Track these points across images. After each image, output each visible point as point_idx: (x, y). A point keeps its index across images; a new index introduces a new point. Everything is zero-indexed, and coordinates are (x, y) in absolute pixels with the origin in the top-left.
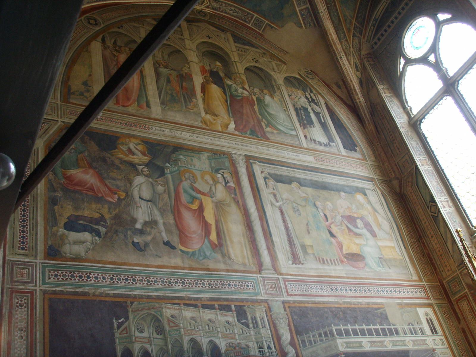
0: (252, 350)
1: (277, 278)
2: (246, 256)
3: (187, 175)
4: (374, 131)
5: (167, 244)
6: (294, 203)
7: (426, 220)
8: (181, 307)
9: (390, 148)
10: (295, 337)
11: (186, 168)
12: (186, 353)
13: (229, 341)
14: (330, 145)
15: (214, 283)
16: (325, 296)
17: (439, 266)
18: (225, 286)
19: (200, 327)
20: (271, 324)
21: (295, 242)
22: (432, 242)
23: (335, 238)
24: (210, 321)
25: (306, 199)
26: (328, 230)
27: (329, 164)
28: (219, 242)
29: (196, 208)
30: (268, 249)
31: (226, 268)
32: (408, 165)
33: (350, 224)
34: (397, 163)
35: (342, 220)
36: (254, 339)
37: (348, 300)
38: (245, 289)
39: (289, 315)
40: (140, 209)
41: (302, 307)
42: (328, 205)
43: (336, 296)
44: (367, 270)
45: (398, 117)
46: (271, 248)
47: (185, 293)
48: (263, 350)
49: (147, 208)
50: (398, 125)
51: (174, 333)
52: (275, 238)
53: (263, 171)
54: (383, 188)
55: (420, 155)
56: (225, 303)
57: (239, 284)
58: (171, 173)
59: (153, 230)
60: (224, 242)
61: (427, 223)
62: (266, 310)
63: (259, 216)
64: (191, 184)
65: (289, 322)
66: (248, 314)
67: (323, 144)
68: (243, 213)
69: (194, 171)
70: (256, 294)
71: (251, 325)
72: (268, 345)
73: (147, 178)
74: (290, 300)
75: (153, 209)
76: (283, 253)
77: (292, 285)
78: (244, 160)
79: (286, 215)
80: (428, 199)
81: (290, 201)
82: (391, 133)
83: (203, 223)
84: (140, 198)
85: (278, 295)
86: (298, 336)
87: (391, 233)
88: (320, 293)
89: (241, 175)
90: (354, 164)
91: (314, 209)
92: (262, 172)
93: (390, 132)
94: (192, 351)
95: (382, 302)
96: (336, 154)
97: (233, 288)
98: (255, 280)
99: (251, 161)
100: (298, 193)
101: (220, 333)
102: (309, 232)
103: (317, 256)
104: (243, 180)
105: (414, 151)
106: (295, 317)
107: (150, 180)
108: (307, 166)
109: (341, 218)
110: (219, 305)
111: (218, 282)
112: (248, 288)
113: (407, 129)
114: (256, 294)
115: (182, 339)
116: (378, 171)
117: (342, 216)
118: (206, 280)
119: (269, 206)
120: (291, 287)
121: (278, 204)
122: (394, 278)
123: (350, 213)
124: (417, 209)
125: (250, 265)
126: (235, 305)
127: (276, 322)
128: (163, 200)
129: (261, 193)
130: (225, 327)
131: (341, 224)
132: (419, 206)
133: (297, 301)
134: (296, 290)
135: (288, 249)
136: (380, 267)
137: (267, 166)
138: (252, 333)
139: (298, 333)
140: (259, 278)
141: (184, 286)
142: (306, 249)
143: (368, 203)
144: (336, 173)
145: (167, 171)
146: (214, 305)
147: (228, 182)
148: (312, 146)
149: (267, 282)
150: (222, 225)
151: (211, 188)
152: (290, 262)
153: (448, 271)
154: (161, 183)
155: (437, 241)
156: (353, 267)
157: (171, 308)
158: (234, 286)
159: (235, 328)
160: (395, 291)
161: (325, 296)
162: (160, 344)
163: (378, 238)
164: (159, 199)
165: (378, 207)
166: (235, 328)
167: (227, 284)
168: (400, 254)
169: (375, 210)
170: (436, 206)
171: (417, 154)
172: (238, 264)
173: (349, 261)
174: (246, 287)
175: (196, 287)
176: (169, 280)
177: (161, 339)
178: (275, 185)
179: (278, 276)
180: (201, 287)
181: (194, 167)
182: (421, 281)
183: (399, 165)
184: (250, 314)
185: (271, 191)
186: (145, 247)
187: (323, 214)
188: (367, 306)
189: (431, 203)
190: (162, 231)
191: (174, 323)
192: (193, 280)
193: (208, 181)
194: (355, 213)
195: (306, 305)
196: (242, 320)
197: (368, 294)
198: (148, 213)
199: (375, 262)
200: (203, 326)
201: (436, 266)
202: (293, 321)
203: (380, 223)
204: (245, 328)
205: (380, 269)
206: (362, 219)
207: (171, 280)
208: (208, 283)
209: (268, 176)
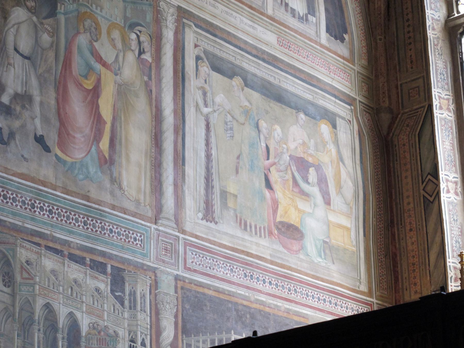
0: (121, 341)
1: (176, 236)
2: (143, 190)
3: (88, 23)
4: (383, 12)
5: (40, 140)
6: (229, 113)
7: (411, 199)
8: (41, 250)
9: (398, 54)
10: (180, 337)
11: (88, 10)
12: (36, 324)
13: (94, 319)
14: (307, 20)
15: (92, 223)
16: (234, 283)
17: (404, 281)
18: (105, 231)
19: (61, 288)
20: (153, 308)
21: (214, 183)
22: (408, 238)
23: (271, 191)
24: (75, 283)
25: (247, 112)
27: (295, 56)
28: (110, 156)
29: (90, 88)
30: (176, 185)
31: (112, 202)
32: (417, 96)
33: (299, 173)
34: (401, 85)
36: (126, 325)
37: (263, 298)
38: (131, 243)
39: (180, 300)
40: (12, 69)
41: (198, 292)
42: (275, 130)
43: (248, 288)
44: (302, 256)
45: (433, 6)
46: (179, 184)
47: (50, 228)
48: (135, 345)
49: (23, 70)
50: (427, 21)
51: (26, 290)
52: (189, 170)
53: (198, 44)
54: (364, 122)
55: (442, 88)
56: (101, 259)
57: (124, 233)
58: (65, 14)
59: (25, 111)
60: (117, 158)
61: (412, 205)
62: (151, 284)
63: (174, 125)
64: (90, 42)
65: (177, 311)
66: (127, 284)
67: (297, 16)
68: (154, 114)
69: (99, 18)
70: (144, 255)
71: (127, 303)
72: (143, 340)
73: (30, 14)
74: (186, 278)
75: (30, 74)
76: (194, 197)
77: (194, 253)
78: (175, 17)
79: (212, 134)
80: (428, 167)
81: (225, 109)
82: (411, 29)
83: (94, 116)
84: (16, 50)
85: (172, 264)
86: (184, 336)
87: (353, 204)
88: (229, 276)
89: (165, 44)
90: (334, 65)
91: (254, 134)
92: (196, 46)
93: (409, 26)
94: (44, 324)
95: (307, 314)
96: (311, 40)
97: (115, 238)
98: (147, 231)
100: (239, 97)
101: (84, 305)
102: (237, 172)
103: (239, 215)
104: (165, 54)
105: (437, 78)
106: (187, 306)
107: (35, 19)
108: (264, 52)
109: (288, 158)
110: (91, 260)
111: (97, 222)
112: (135, 243)
113: (438, 35)
114: (144, 255)
115: (34, 301)
116: (365, 88)
117: (290, 156)
118: (82, 214)
119: (193, 110)
120: (193, 256)
121: (206, 110)
122: (335, 280)
123: (304, 153)
124: (404, 175)
125: (145, 206)
126: (112, 266)
127: (160, 306)
128: (46, 61)
129: (187, 84)
130: (93, 296)
131: (287, 170)
132: (409, 173)
133: (195, 280)
134: (198, 263)
135: (203, 192)
137: (206, 37)
138: (126, 315)
139: (186, 332)
140: (153, 229)
141: (51, 216)
142: (226, 200)
143: (333, 143)
144: (302, 76)
145: (61, 9)
146: (84, 258)
147: (144, 52)
148: (281, 15)
149: (162, 241)
150: (121, 127)
151: (117, 56)
152: (200, 215)
153: (416, 292)
154: (49, 28)
155: (416, 239)
156: (284, 247)
157: (28, 249)
158: (116, 235)
159: (105, 301)
160: (330, 302)
161: (234, 283)
162: (5, 301)
163: (332, 208)
164: (41, 59)
165: (347, 154)
166: (105, 301)
167: (109, 228)
168: (354, 243)
169: (341, 159)
170: (437, 185)
171: (440, 84)
172: (129, 199)
173: (281, 236)
174: (132, 240)
175: (66, 222)
176: (33, 202)
177: (8, 294)
178: (209, 75)
179: (178, 234)
180: (72, 224)
181: (101, 11)
182: (371, 296)
183: (402, 90)
184: (129, 285)
185: (200, 85)
186: (8, 138)
187: (265, 145)
188: (285, 315)
189: (429, 177)
190: (36, 117)
191: (28, 273)
192: (64, 211)
193: (116, 41)
194: (311, 155)
195: (206, 291)
196: (117, 292)
197: (292, 296)
198: (23, 79)
199: (316, 246)
200: (66, 287)
201: (400, 277)
202: (183, 311)
203: (342, 183)
204: (118, 305)
205: (320, 260)
206: (318, 168)
207: (35, 202)
208: (83, 220)
209: (202, 55)
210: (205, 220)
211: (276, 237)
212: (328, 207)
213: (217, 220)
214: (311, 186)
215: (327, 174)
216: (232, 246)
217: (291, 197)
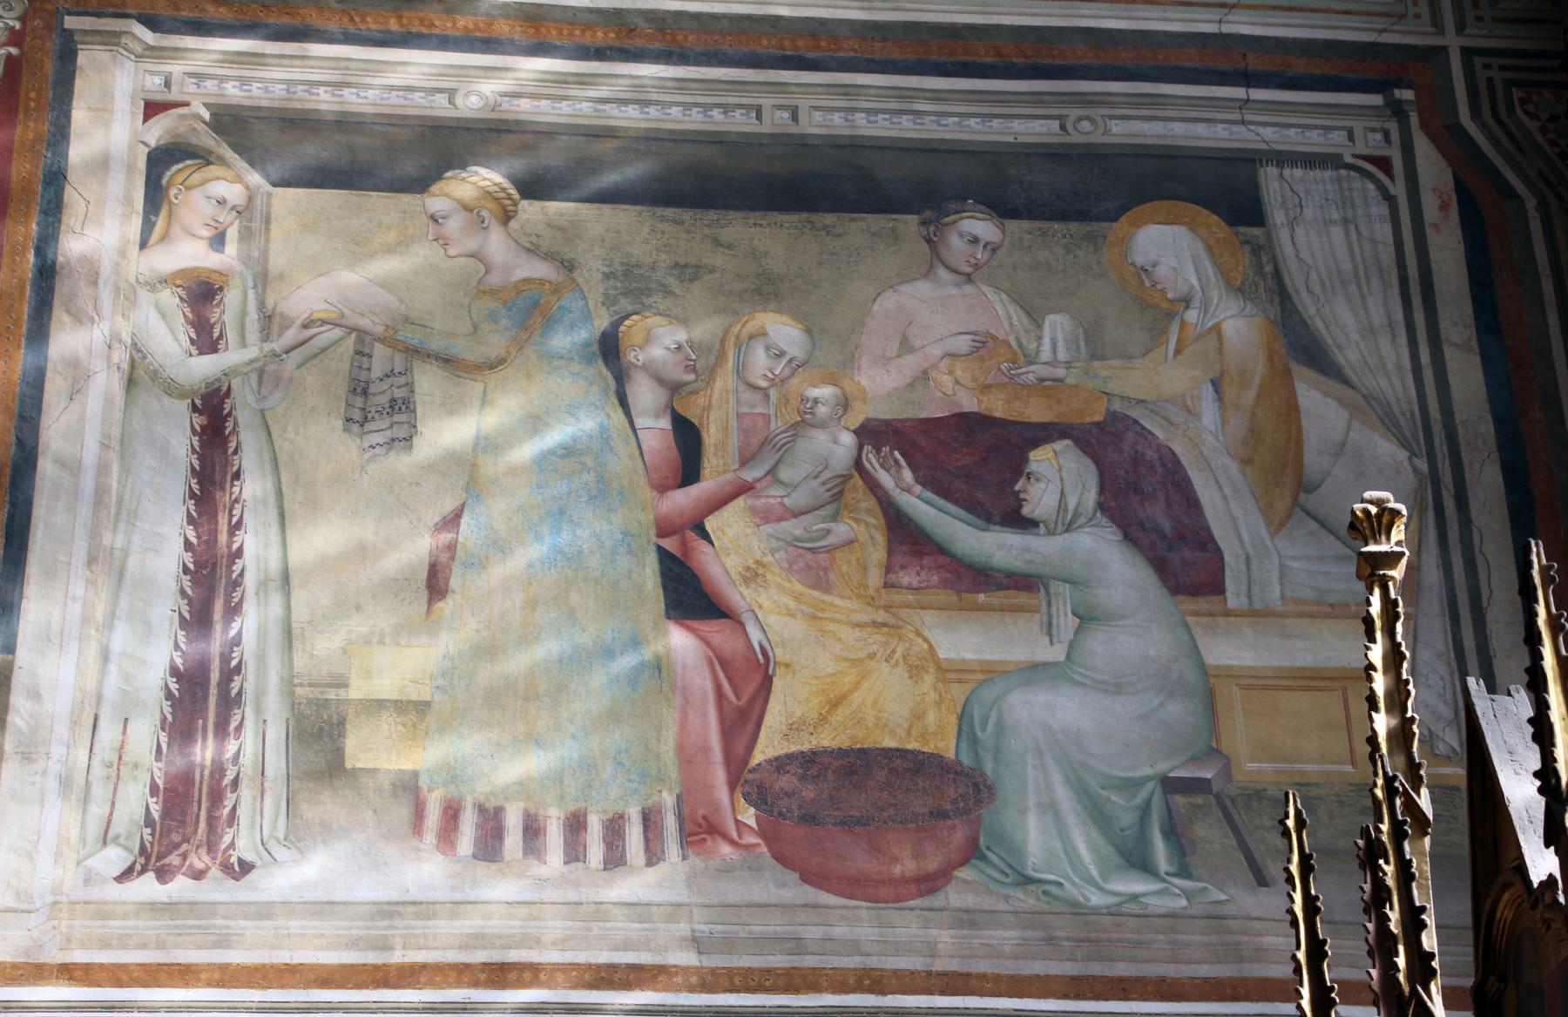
23: (713, 628)
26: (664, 555)
35: (858, 464)
99: (70, 22)
136: (1141, 863)
152: (115, 858)
163: (1234, 596)
187: (665, 423)
203: (1314, 460)
205: (1138, 885)
209: (208, 140)
210: (151, 876)
211: (752, 839)
212: (1203, 604)
213: (249, 857)
214: (1051, 533)
215: (1178, 448)
216: (372, 958)
217: (881, 616)
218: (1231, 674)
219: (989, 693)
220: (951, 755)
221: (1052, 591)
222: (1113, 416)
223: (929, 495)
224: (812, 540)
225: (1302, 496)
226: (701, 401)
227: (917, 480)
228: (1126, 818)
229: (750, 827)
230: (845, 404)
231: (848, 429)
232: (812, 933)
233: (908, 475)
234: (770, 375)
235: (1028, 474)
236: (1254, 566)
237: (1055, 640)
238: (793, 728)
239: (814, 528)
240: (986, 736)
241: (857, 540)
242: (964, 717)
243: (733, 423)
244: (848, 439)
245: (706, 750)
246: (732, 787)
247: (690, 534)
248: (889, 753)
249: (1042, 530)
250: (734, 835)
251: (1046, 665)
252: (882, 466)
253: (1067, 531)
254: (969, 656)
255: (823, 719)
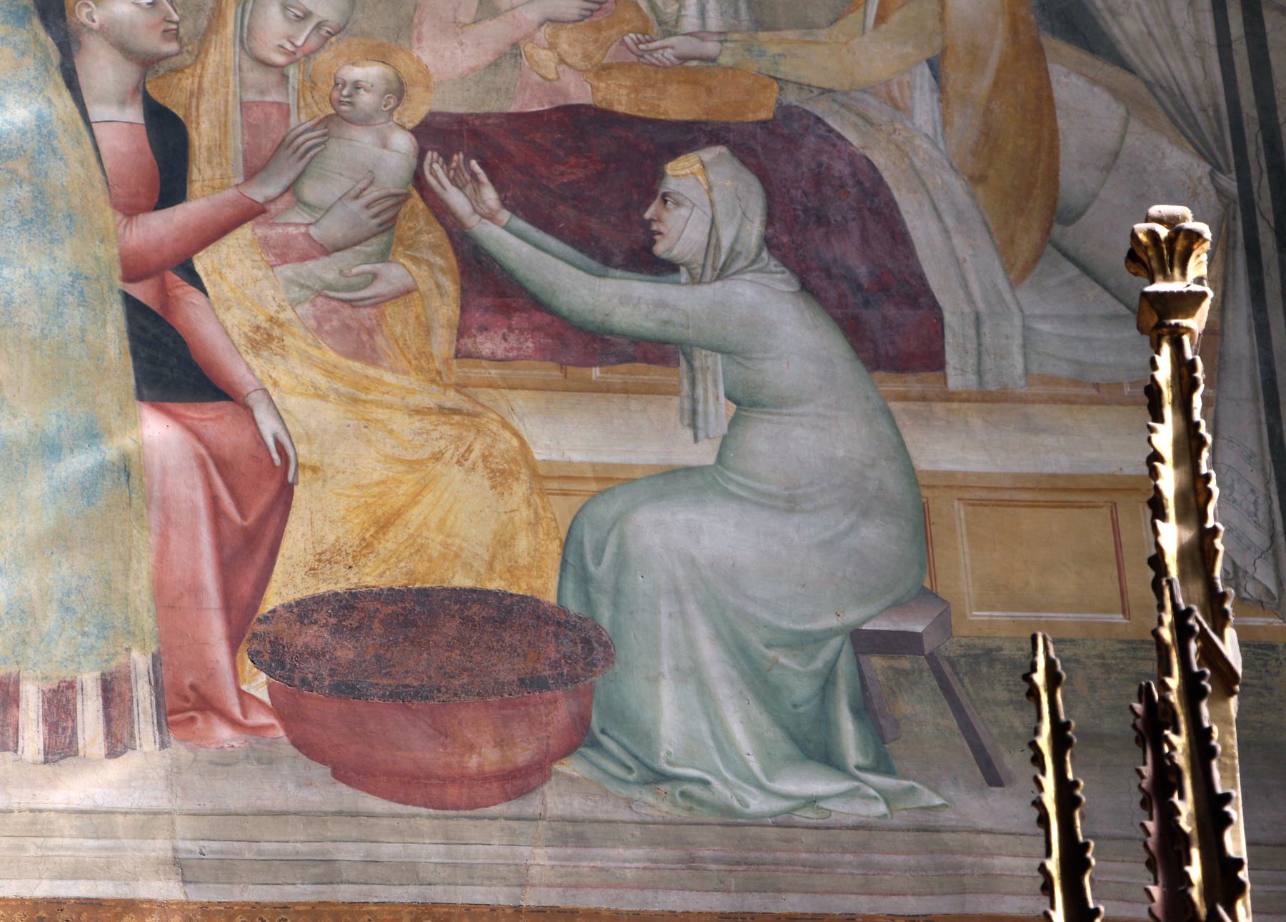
23: (208, 415)
26: (133, 307)
35: (418, 179)
163: (958, 375)
187: (134, 114)
205: (818, 784)
212: (913, 383)
214: (696, 280)
215: (879, 160)
218: (951, 483)
219: (606, 510)
220: (551, 598)
221: (697, 364)
222: (786, 113)
223: (521, 225)
224: (350, 288)
225: (1057, 229)
226: (188, 83)
227: (504, 203)
228: (802, 689)
229: (261, 702)
230: (398, 91)
231: (403, 127)
232: (349, 852)
233: (490, 195)
234: (289, 46)
235: (664, 195)
236: (986, 329)
237: (701, 434)
238: (323, 560)
239: (355, 271)
240: (601, 571)
241: (416, 289)
242: (570, 544)
243: (235, 116)
244: (403, 142)
245: (195, 590)
246: (234, 644)
247: (173, 278)
248: (462, 596)
249: (684, 275)
250: (237, 712)
251: (689, 470)
252: (453, 181)
253: (719, 278)
254: (577, 457)
255: (366, 546)
